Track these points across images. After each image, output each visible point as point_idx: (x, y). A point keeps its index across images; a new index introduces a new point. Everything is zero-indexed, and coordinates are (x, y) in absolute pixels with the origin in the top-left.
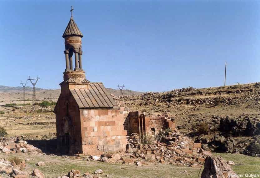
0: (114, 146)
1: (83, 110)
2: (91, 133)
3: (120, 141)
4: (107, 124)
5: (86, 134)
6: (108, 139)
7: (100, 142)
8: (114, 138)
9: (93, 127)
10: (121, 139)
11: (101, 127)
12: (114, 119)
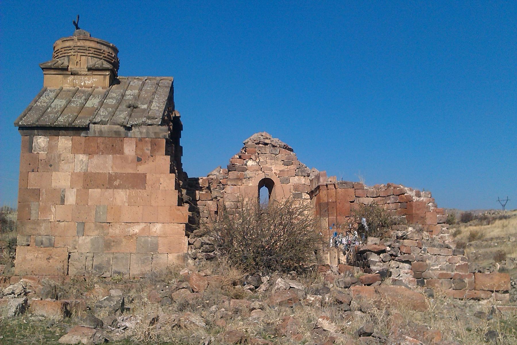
0: (134, 257)
2: (53, 209)
3: (161, 241)
4: (116, 183)
5: (33, 212)
6: (115, 231)
7: (81, 240)
8: (136, 229)
9: (64, 191)
10: (165, 236)
11: (90, 190)
12: (142, 169)
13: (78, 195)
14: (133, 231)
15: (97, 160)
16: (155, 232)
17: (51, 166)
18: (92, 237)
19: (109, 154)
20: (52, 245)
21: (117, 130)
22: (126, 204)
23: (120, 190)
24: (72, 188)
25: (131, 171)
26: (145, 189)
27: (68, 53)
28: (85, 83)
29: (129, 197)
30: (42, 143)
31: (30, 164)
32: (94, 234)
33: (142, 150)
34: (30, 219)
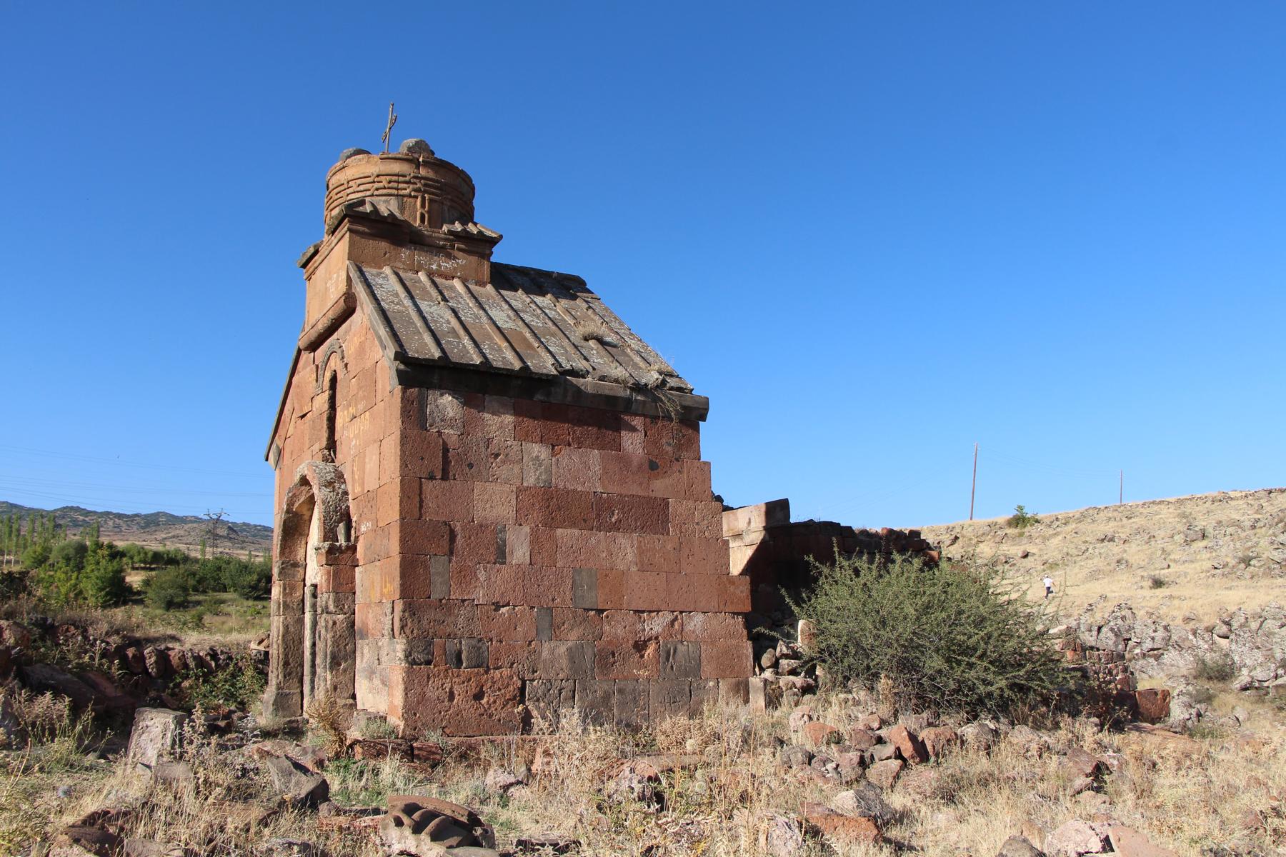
1: (431, 386)
2: (482, 575)
5: (437, 580)
6: (617, 629)
8: (656, 625)
9: (503, 530)
11: (559, 531)
12: (660, 487)
13: (535, 541)
14: (651, 629)
15: (570, 459)
16: (693, 632)
17: (471, 466)
18: (570, 644)
19: (592, 447)
20: (480, 663)
21: (612, 393)
22: (634, 569)
23: (620, 535)
24: (521, 525)
25: (635, 490)
26: (668, 534)
27: (397, 189)
28: (439, 266)
29: (641, 552)
30: (449, 409)
31: (422, 459)
32: (573, 637)
33: (656, 443)
34: (429, 597)
